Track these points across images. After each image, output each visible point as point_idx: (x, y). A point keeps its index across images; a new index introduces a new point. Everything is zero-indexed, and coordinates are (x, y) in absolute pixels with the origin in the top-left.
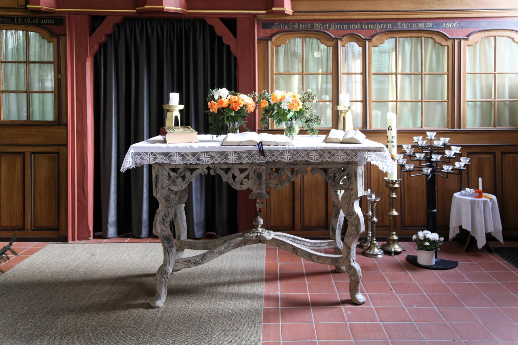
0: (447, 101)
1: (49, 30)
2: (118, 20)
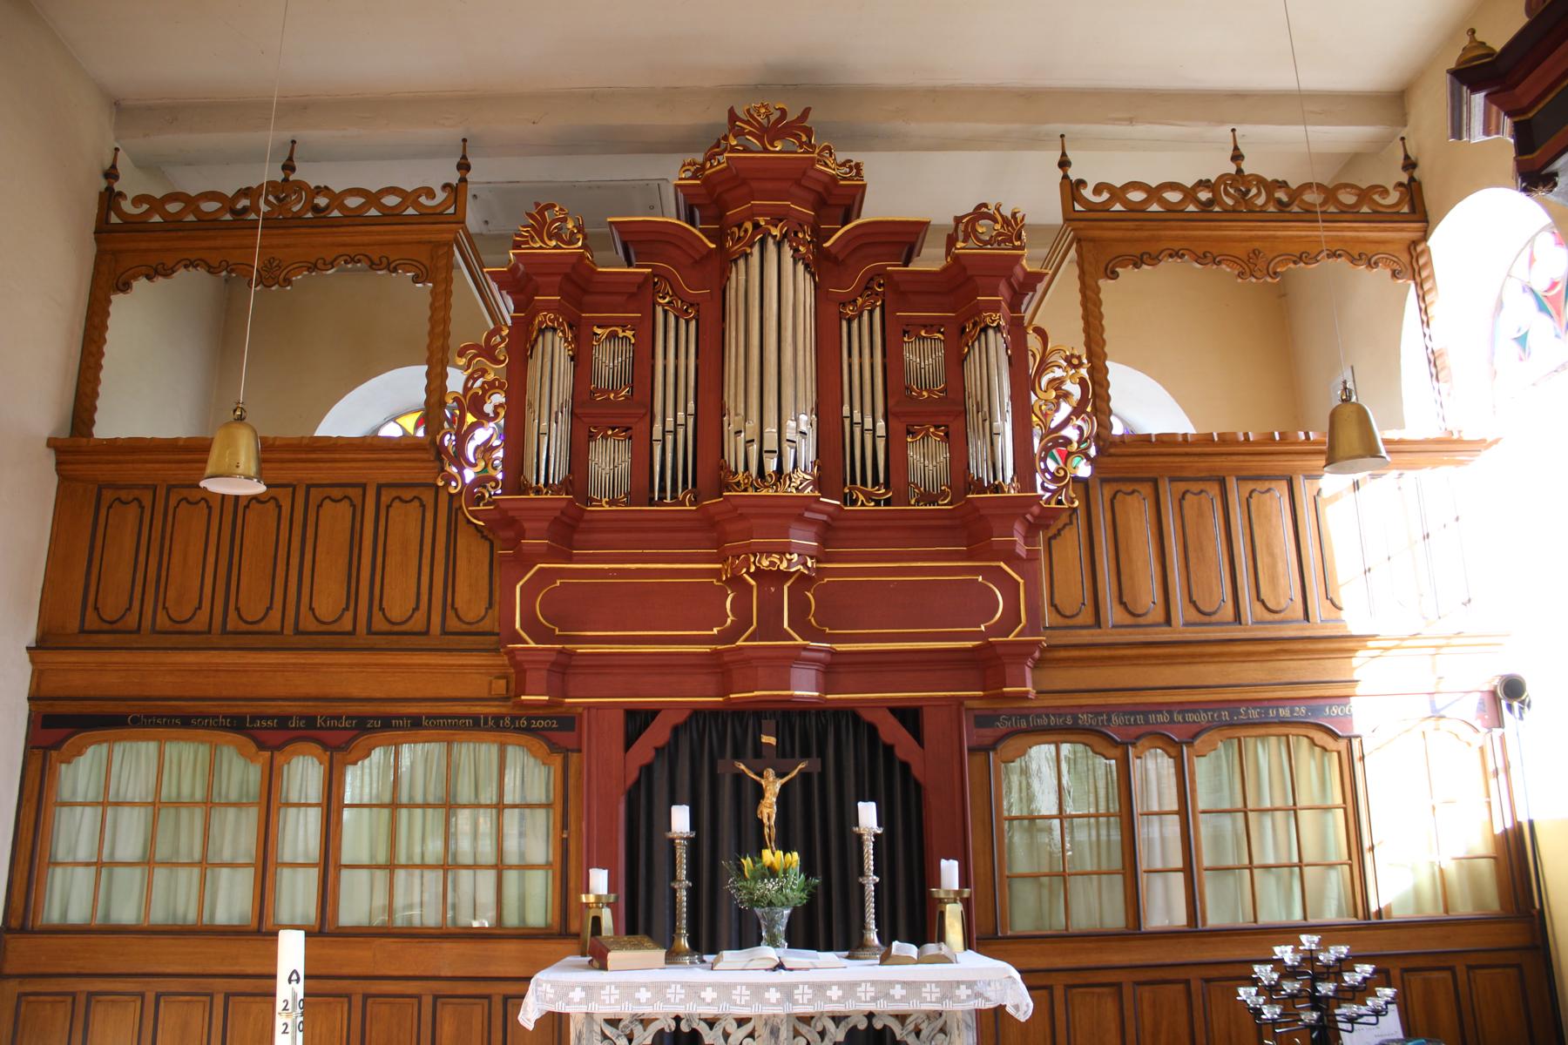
0: (1350, 862)
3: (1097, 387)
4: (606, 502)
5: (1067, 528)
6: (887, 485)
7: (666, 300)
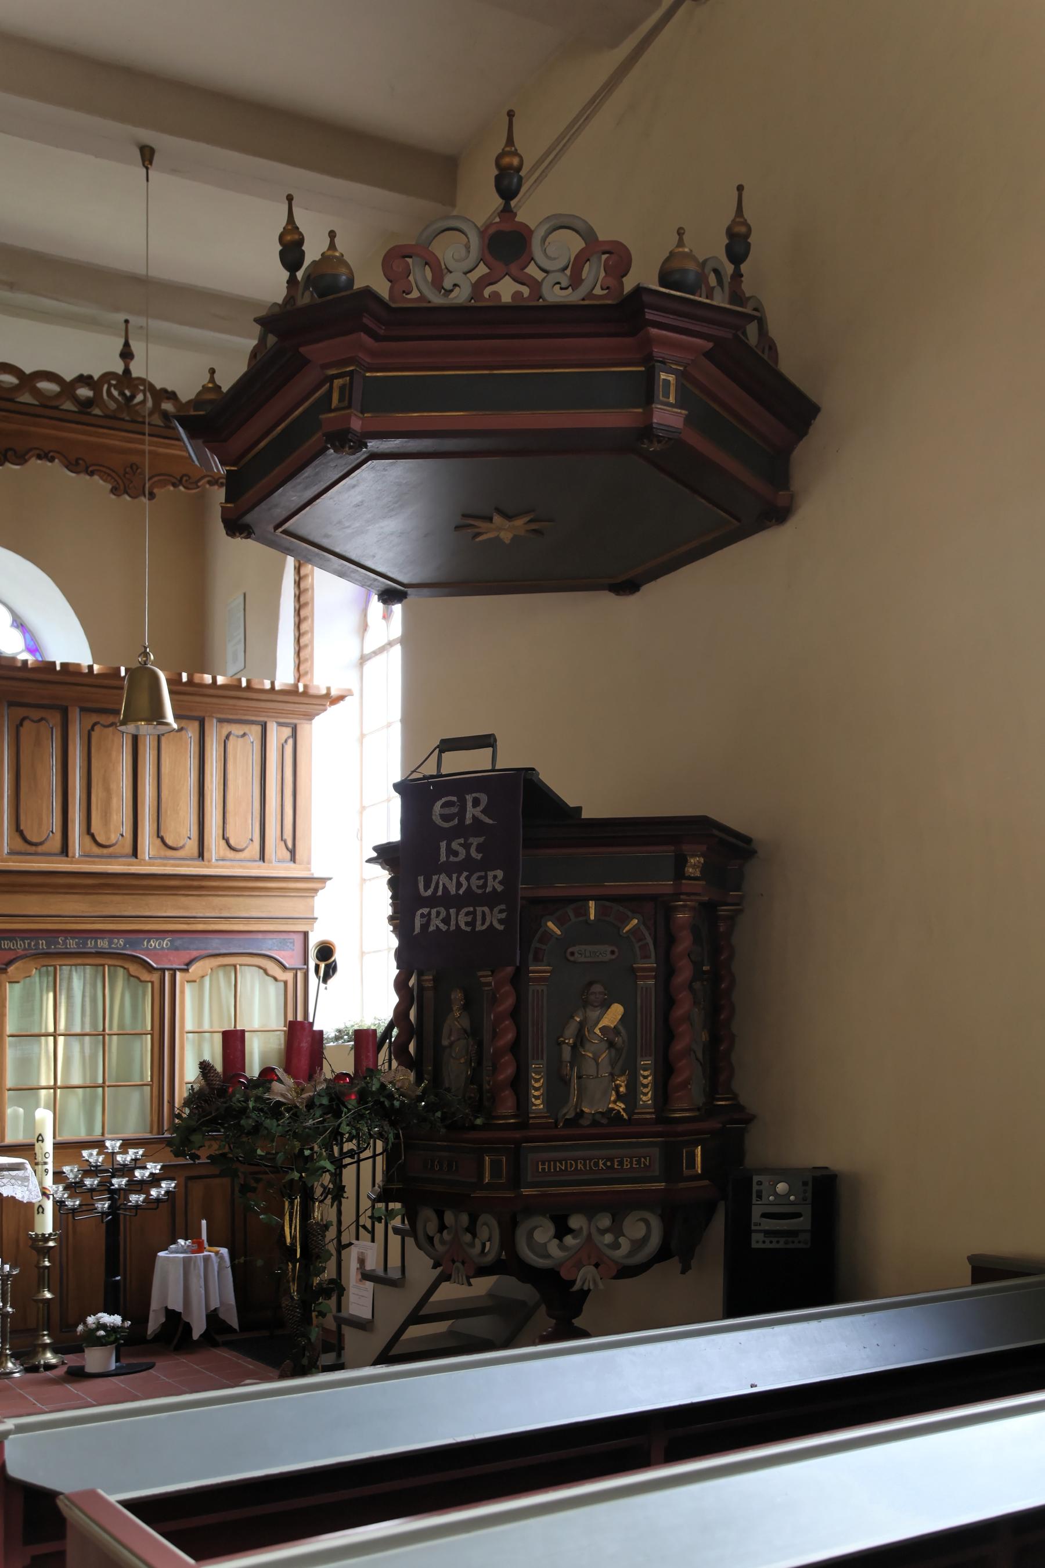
0: (151, 1083)
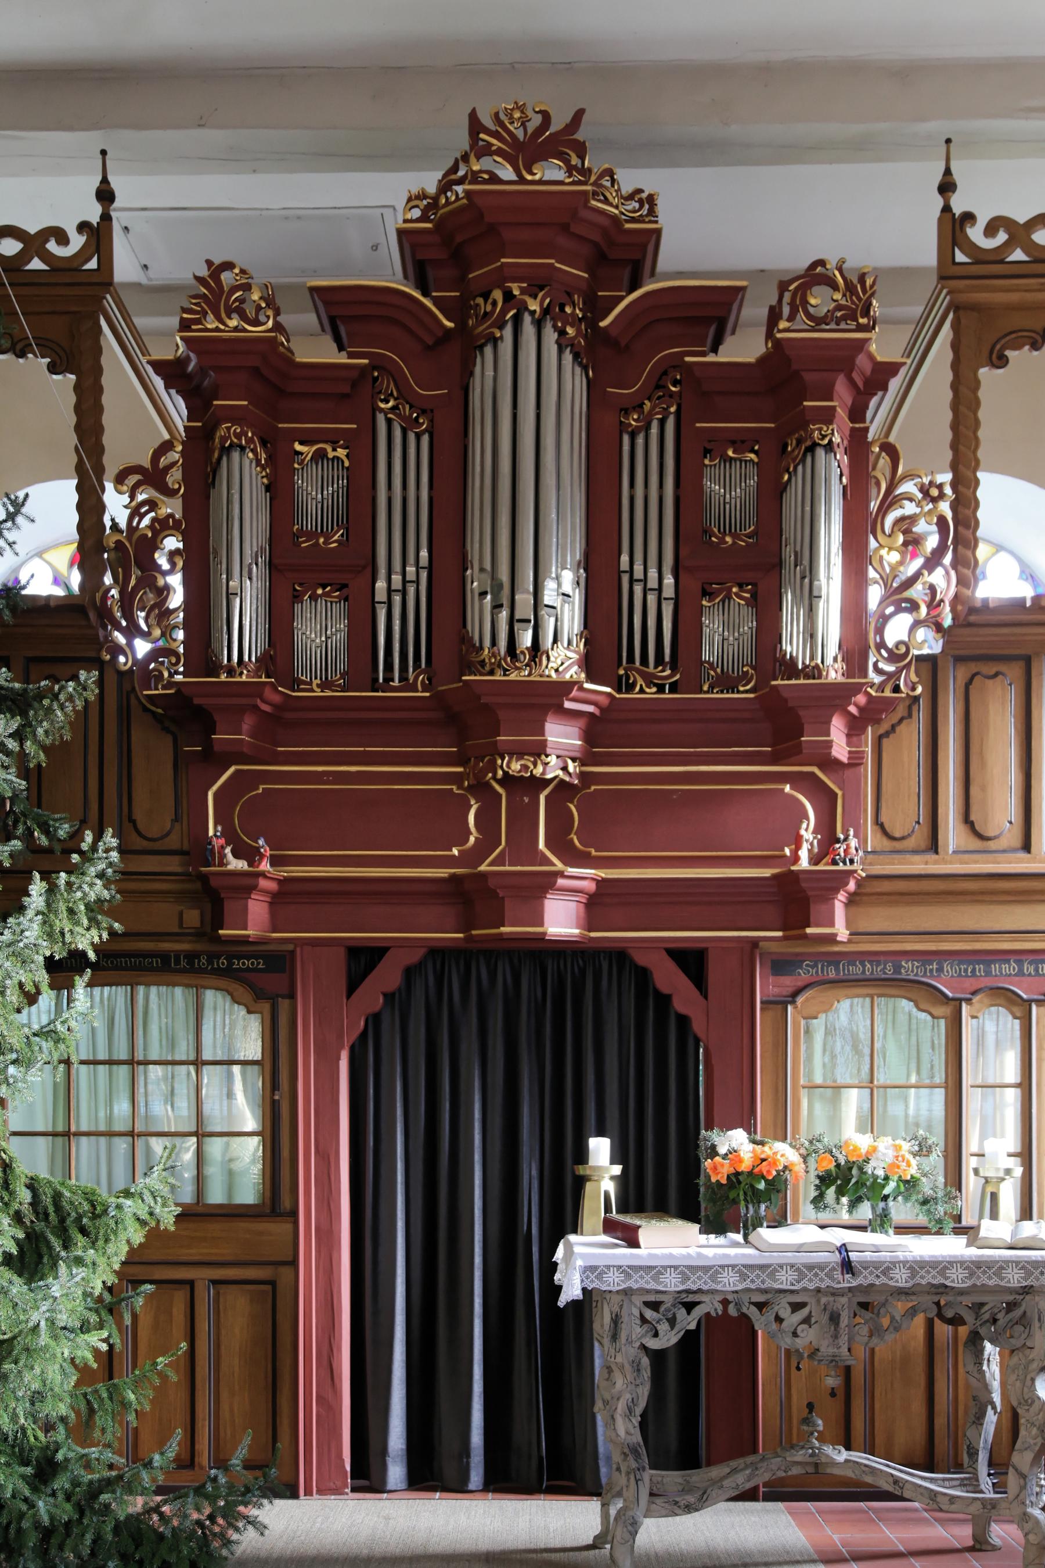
1: (251, 986)
2: (415, 956)
3: (960, 528)
4: (317, 685)
5: (905, 722)
6: (674, 665)
7: (391, 404)
